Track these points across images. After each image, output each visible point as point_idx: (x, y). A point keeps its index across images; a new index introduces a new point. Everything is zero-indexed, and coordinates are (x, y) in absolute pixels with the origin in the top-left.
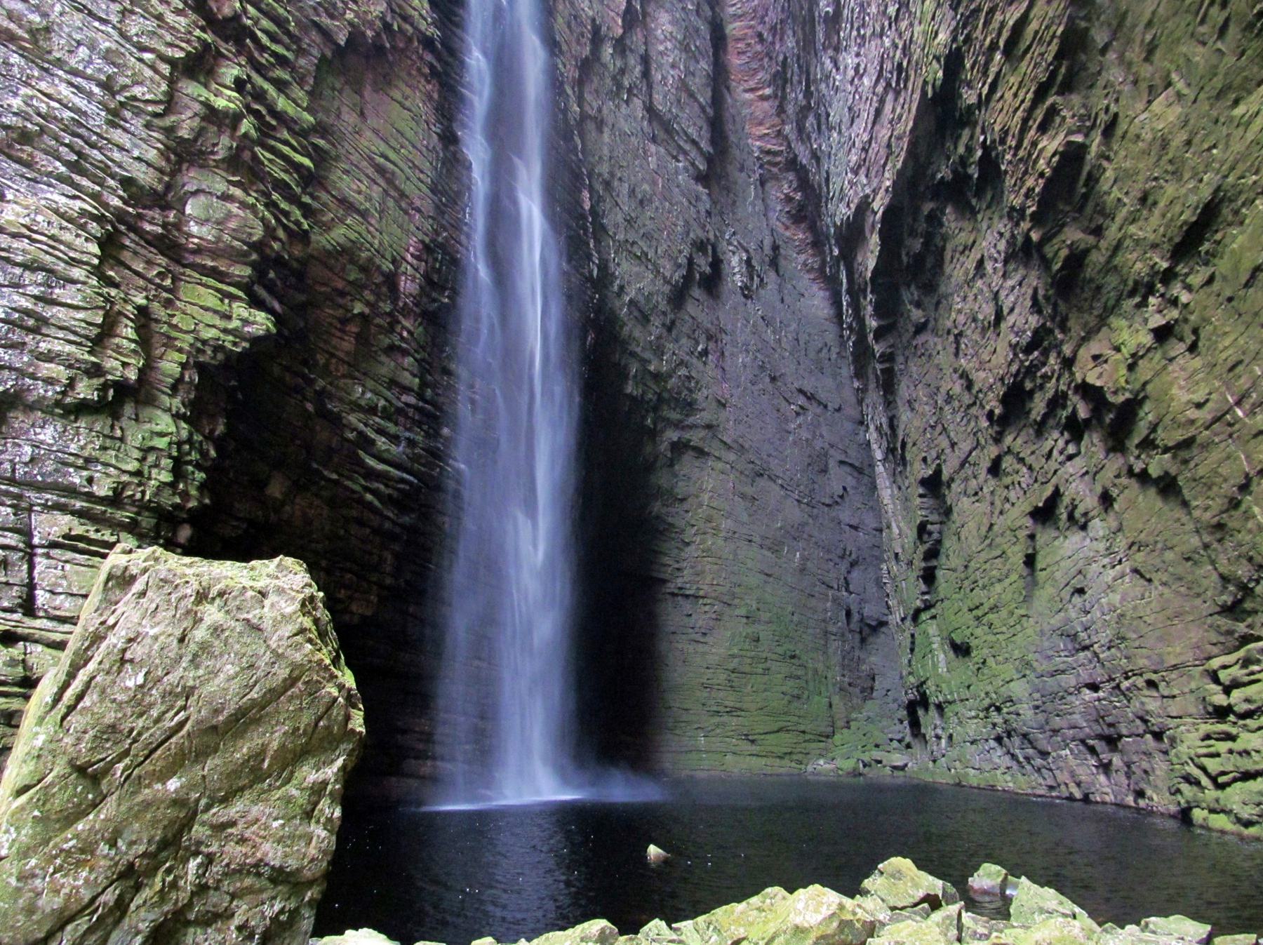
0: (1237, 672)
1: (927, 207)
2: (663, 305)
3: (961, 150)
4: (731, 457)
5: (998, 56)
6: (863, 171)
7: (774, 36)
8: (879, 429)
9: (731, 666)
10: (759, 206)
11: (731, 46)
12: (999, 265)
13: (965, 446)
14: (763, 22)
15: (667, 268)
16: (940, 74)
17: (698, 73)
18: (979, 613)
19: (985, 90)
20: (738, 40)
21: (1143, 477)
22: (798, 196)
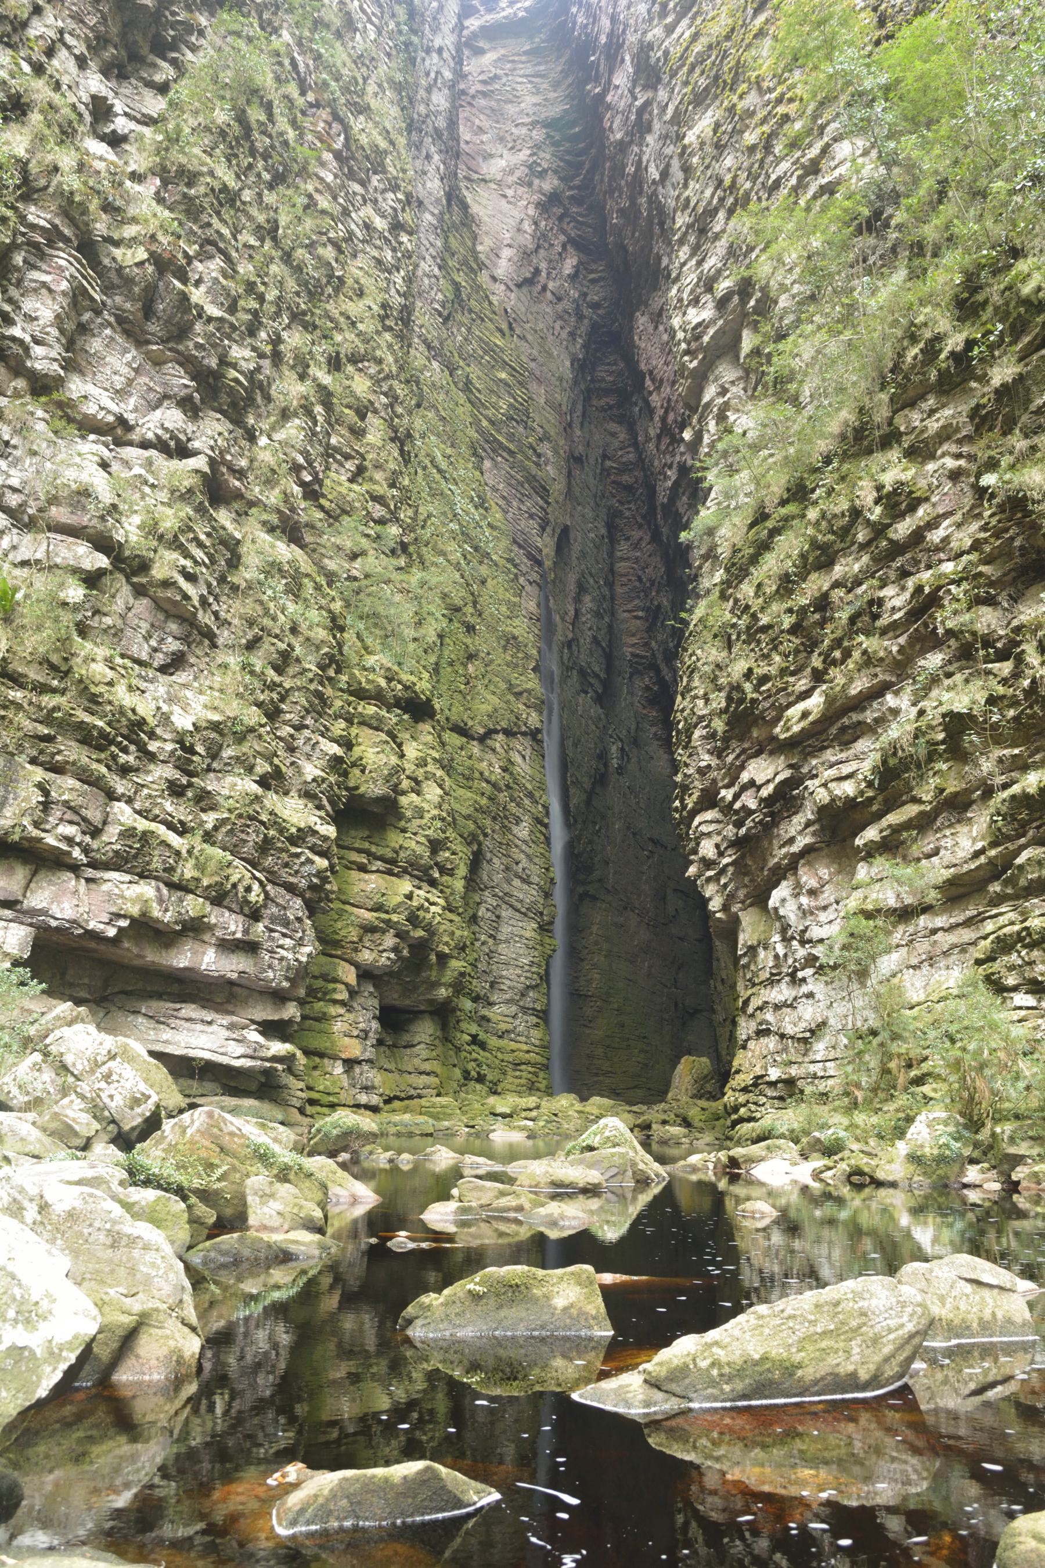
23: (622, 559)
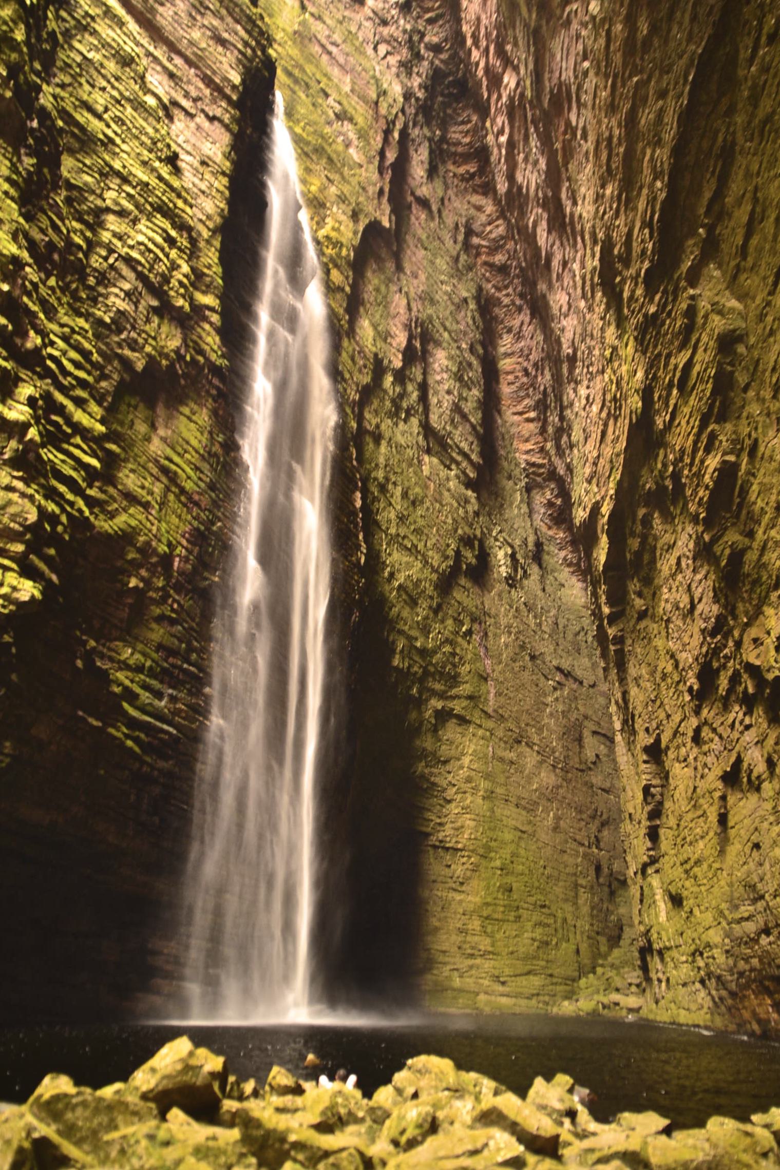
1: (641, 512)
2: (430, 590)
3: (659, 466)
4: (490, 724)
5: (675, 392)
6: (594, 481)
7: (537, 371)
9: (485, 914)
10: (524, 509)
11: (504, 380)
12: (690, 562)
13: (677, 718)
14: (528, 359)
15: (435, 559)
16: (640, 404)
17: (470, 398)
18: (688, 866)
20: (508, 373)
22: (559, 502)
23: (507, 355)
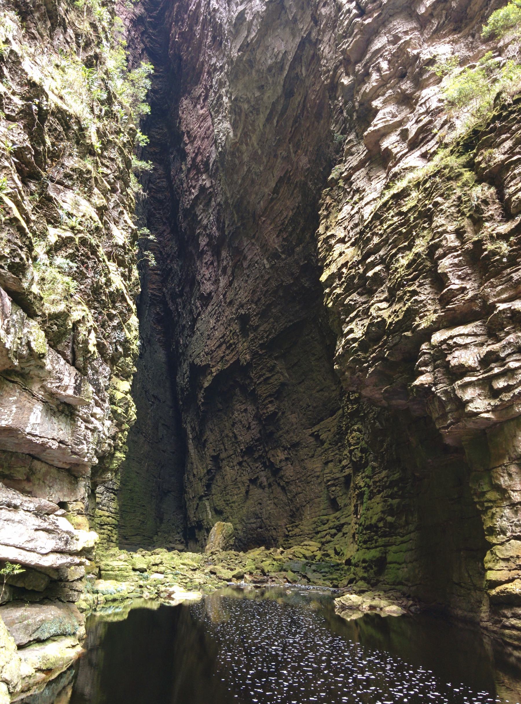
0: (291, 529)
8: (193, 429)
13: (231, 452)
14: (163, 247)
19: (258, 382)
21: (279, 484)
